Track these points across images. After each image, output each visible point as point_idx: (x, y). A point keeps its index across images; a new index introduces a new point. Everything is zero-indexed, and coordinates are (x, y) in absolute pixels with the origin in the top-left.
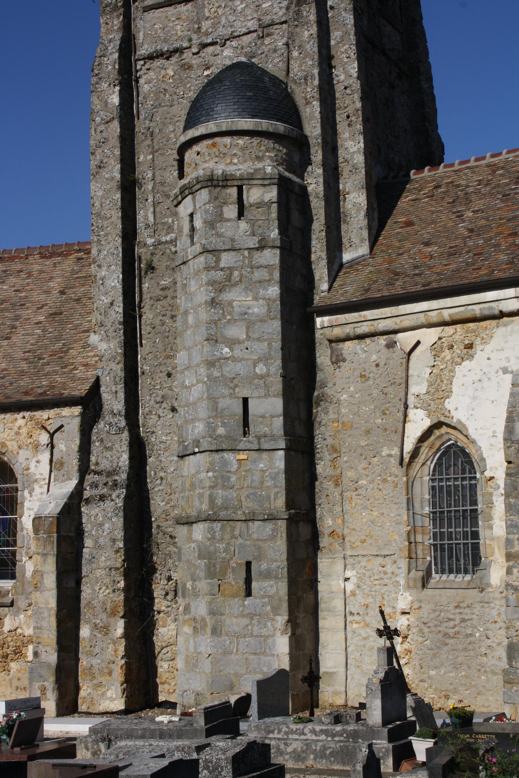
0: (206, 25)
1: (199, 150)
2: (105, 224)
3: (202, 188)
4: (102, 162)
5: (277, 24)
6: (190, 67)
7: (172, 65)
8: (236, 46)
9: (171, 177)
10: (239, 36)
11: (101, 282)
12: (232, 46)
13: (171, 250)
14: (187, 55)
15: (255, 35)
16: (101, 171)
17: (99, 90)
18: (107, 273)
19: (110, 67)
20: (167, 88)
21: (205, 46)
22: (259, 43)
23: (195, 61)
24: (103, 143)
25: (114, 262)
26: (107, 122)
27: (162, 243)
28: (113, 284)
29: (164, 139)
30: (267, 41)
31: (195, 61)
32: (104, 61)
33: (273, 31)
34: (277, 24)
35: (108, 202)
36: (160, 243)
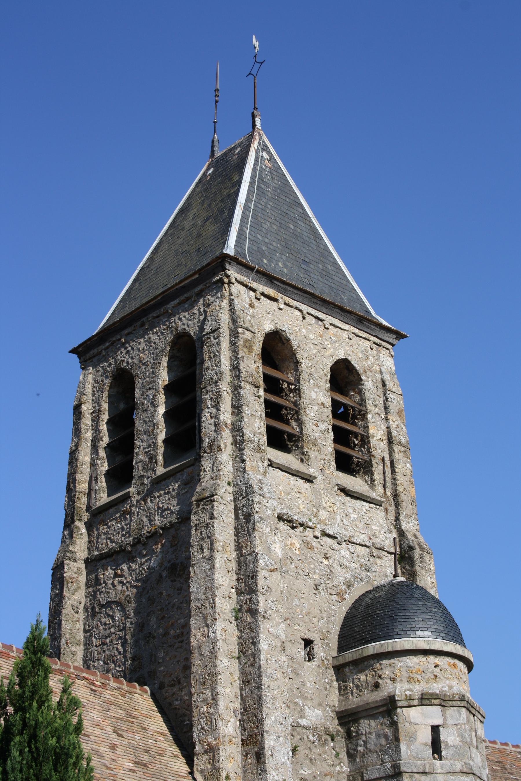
0: (324, 515)
1: (439, 663)
2: (272, 684)
3: (464, 707)
4: (265, 612)
5: (386, 551)
6: (312, 548)
7: (296, 536)
8: (352, 551)
9: (299, 655)
10: (354, 543)
11: (270, 753)
12: (348, 549)
13: (308, 738)
14: (309, 533)
15: (367, 550)
16: (265, 621)
17: (261, 530)
18: (275, 744)
19: (270, 512)
20: (293, 557)
21: (325, 534)
22: (372, 559)
23: (315, 543)
24: (266, 591)
25: (283, 733)
26: (272, 571)
27: (301, 726)
28: (283, 760)
29: (291, 611)
30: (378, 561)
31: (315, 543)
32: (263, 501)
33: (381, 555)
34: (386, 551)
35: (274, 661)
36: (299, 726)
